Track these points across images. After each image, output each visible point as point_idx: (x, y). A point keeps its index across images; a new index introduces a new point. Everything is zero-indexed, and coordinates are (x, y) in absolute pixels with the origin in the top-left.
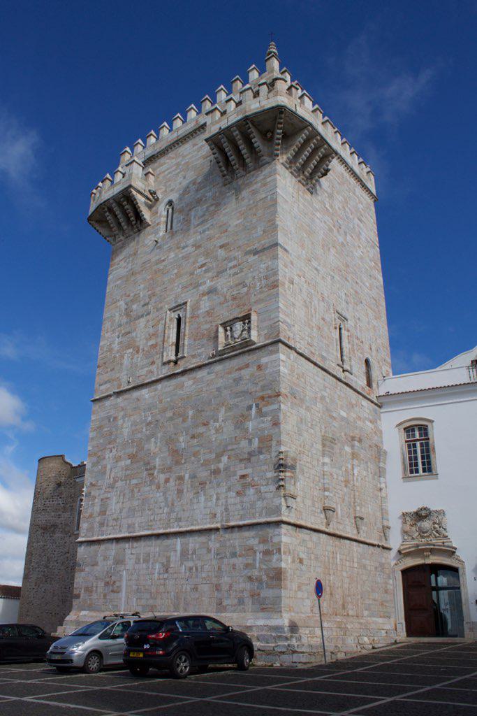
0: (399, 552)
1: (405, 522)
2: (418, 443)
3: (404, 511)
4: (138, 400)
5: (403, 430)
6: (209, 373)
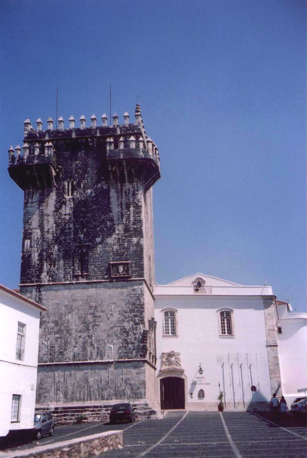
0: (160, 371)
2: (170, 320)
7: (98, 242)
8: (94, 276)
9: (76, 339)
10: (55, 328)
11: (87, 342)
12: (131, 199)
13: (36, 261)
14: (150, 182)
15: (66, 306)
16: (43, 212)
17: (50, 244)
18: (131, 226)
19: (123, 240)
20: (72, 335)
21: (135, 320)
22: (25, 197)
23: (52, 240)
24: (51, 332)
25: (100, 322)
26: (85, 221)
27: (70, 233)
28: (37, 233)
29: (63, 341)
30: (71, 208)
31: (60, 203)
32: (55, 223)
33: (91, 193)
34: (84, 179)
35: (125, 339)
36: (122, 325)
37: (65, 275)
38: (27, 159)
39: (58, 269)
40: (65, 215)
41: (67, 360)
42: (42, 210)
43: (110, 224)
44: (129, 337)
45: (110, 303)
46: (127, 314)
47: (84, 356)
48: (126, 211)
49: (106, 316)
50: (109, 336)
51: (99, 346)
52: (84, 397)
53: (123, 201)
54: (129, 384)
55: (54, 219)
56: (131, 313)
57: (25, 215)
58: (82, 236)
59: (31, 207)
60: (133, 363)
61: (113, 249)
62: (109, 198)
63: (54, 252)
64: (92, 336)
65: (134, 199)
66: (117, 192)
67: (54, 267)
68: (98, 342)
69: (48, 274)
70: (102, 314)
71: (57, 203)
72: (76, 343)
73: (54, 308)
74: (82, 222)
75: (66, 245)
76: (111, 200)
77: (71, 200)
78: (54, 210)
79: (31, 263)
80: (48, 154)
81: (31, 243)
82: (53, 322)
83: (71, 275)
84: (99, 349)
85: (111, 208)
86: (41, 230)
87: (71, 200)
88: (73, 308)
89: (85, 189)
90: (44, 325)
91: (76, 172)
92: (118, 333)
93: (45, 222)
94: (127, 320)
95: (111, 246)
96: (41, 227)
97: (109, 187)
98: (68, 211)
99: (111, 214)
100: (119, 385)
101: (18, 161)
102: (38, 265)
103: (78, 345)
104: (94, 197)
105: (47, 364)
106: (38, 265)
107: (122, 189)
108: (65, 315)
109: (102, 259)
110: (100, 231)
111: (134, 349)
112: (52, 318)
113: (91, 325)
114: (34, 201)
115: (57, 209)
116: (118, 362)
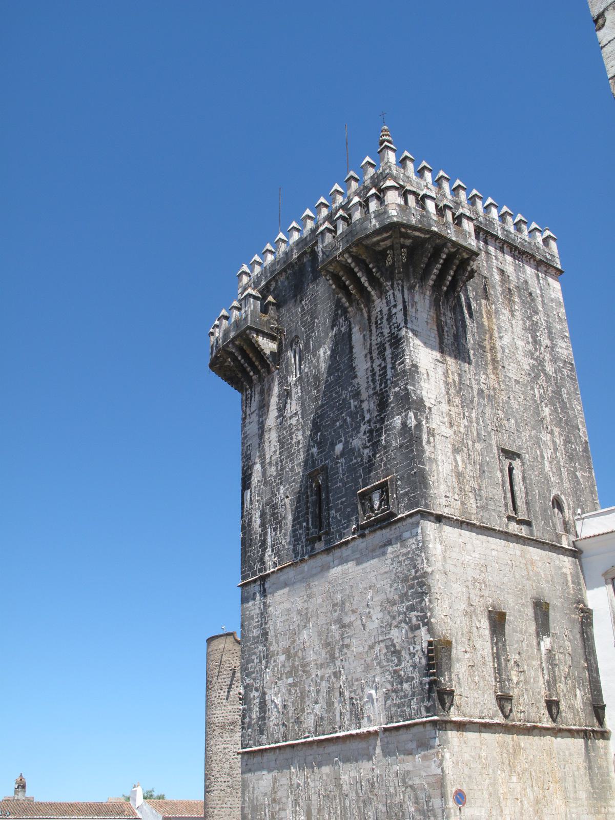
6: (353, 552)
7: (339, 454)
10: (287, 664)
15: (299, 612)
19: (377, 431)
21: (410, 619)
22: (242, 409)
24: (282, 674)
27: (298, 450)
29: (298, 691)
30: (298, 398)
33: (325, 353)
34: (313, 332)
35: (395, 671)
36: (388, 637)
41: (307, 734)
44: (403, 665)
45: (365, 588)
46: (395, 608)
49: (359, 622)
50: (367, 668)
51: (353, 695)
53: (374, 343)
54: (411, 787)
56: (403, 602)
57: (243, 444)
59: (250, 423)
60: (414, 730)
61: (362, 460)
62: (351, 348)
65: (390, 327)
66: (362, 330)
71: (279, 400)
78: (277, 414)
83: (302, 542)
85: (354, 368)
87: (298, 383)
88: (309, 615)
92: (382, 657)
94: (395, 623)
95: (359, 455)
97: (350, 325)
99: (355, 382)
100: (392, 790)
106: (261, 536)
107: (369, 317)
109: (346, 489)
110: (341, 427)
111: (413, 695)
112: (284, 643)
114: (252, 411)
116: (386, 730)
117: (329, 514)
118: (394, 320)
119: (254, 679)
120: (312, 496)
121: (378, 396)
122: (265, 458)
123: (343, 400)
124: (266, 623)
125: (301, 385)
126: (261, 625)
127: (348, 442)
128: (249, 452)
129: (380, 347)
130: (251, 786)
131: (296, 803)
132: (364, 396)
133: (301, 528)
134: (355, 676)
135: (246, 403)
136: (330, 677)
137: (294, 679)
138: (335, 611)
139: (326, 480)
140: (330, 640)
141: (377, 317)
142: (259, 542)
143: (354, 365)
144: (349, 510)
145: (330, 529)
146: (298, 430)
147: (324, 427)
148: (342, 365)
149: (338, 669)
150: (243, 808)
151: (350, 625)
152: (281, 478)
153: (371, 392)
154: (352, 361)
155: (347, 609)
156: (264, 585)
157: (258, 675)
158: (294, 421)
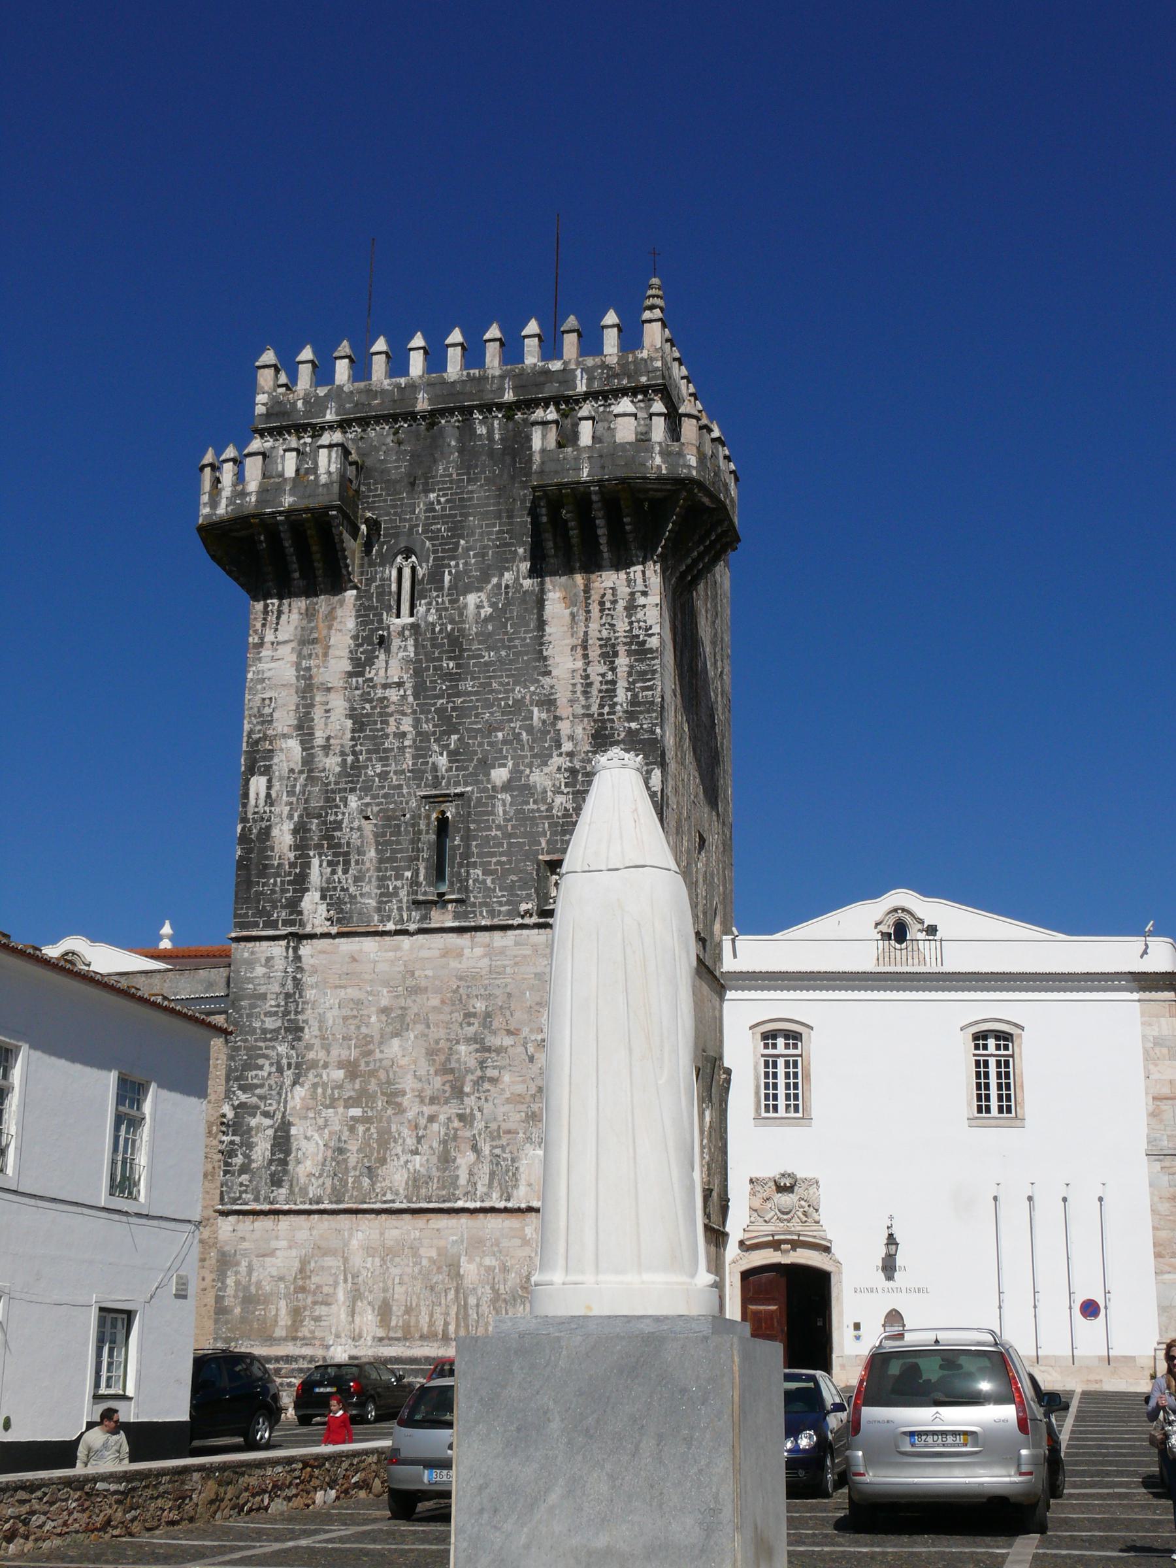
1: (753, 1193)
2: (781, 1062)
3: (753, 1176)
4: (354, 960)
5: (759, 1037)
6: (517, 944)
7: (499, 783)
8: (482, 904)
9: (416, 1127)
11: (455, 1138)
12: (622, 626)
13: (286, 849)
14: (695, 561)
15: (385, 1011)
16: (311, 677)
17: (333, 792)
18: (616, 725)
20: (404, 1111)
23: (339, 774)
25: (501, 1068)
26: (453, 709)
27: (402, 749)
28: (289, 753)
29: (373, 1130)
30: (408, 661)
31: (372, 641)
32: (350, 717)
33: (479, 607)
34: (453, 558)
37: (380, 902)
38: (259, 493)
39: (357, 880)
40: (385, 686)
41: (389, 1197)
42: (309, 669)
43: (544, 716)
47: (444, 1188)
48: (603, 669)
49: (521, 1049)
51: (498, 1151)
52: (446, 1324)
53: (593, 633)
55: (349, 700)
58: (443, 761)
59: (273, 659)
61: (550, 809)
62: (541, 624)
63: (346, 821)
64: (472, 1114)
65: (631, 623)
66: (570, 601)
67: (345, 872)
68: (493, 1139)
69: (323, 897)
70: (508, 1041)
72: (419, 1139)
73: (345, 1018)
74: (441, 711)
75: (385, 796)
76: (548, 629)
77: (407, 633)
78: (350, 668)
79: (269, 858)
80: (329, 473)
81: (269, 788)
82: (340, 1065)
83: (400, 901)
84: (498, 1164)
86: (302, 742)
87: (407, 633)
88: (408, 1019)
89: (461, 587)
90: (311, 1075)
91: (425, 531)
93: (318, 713)
95: (544, 800)
96: (304, 728)
98: (395, 675)
99: (546, 681)
101: (231, 501)
102: (293, 865)
103: (424, 1148)
104: (488, 619)
105: (321, 1207)
107: (587, 590)
108: (381, 1043)
109: (510, 844)
110: (505, 742)
112: (339, 1052)
113: (470, 1077)
114: (281, 638)
115: (360, 666)
117: (468, 872)
118: (640, 615)
119: (261, 1097)
120: (427, 833)
121: (594, 721)
122: (312, 734)
123: (516, 701)
124: (297, 1013)
125: (416, 640)
126: (286, 1013)
127: (522, 772)
128: (267, 711)
129: (606, 646)
130: (244, 1264)
131: (356, 1296)
132: (564, 710)
133: (399, 877)
134: (504, 1126)
135: (265, 619)
136: (449, 1119)
137: (364, 1112)
138: (469, 1024)
139: (465, 818)
140: (453, 1065)
141: (604, 595)
142: (290, 874)
143: (545, 654)
144: (515, 878)
145: (468, 897)
146: (404, 714)
147: (469, 730)
148: (517, 642)
149: (468, 1111)
150: (219, 1299)
151: (499, 1051)
152: (352, 782)
153: (581, 711)
154: (542, 644)
155: (496, 1024)
156: (296, 949)
157: (273, 1093)
158: (393, 695)
